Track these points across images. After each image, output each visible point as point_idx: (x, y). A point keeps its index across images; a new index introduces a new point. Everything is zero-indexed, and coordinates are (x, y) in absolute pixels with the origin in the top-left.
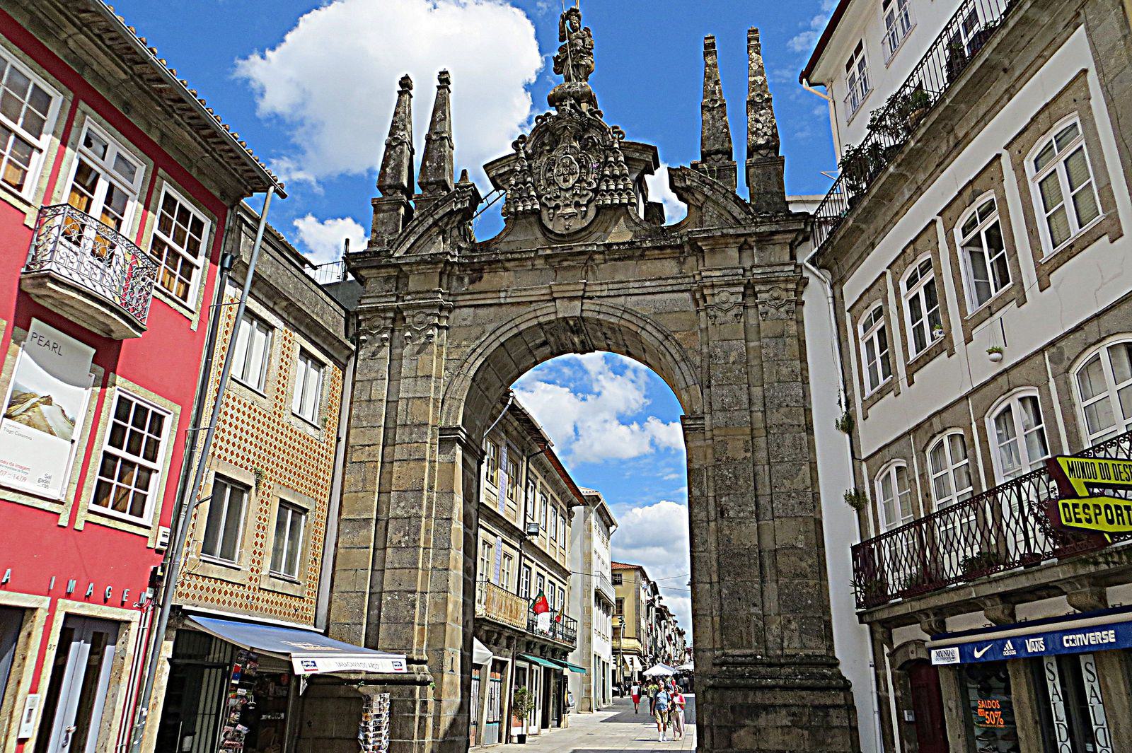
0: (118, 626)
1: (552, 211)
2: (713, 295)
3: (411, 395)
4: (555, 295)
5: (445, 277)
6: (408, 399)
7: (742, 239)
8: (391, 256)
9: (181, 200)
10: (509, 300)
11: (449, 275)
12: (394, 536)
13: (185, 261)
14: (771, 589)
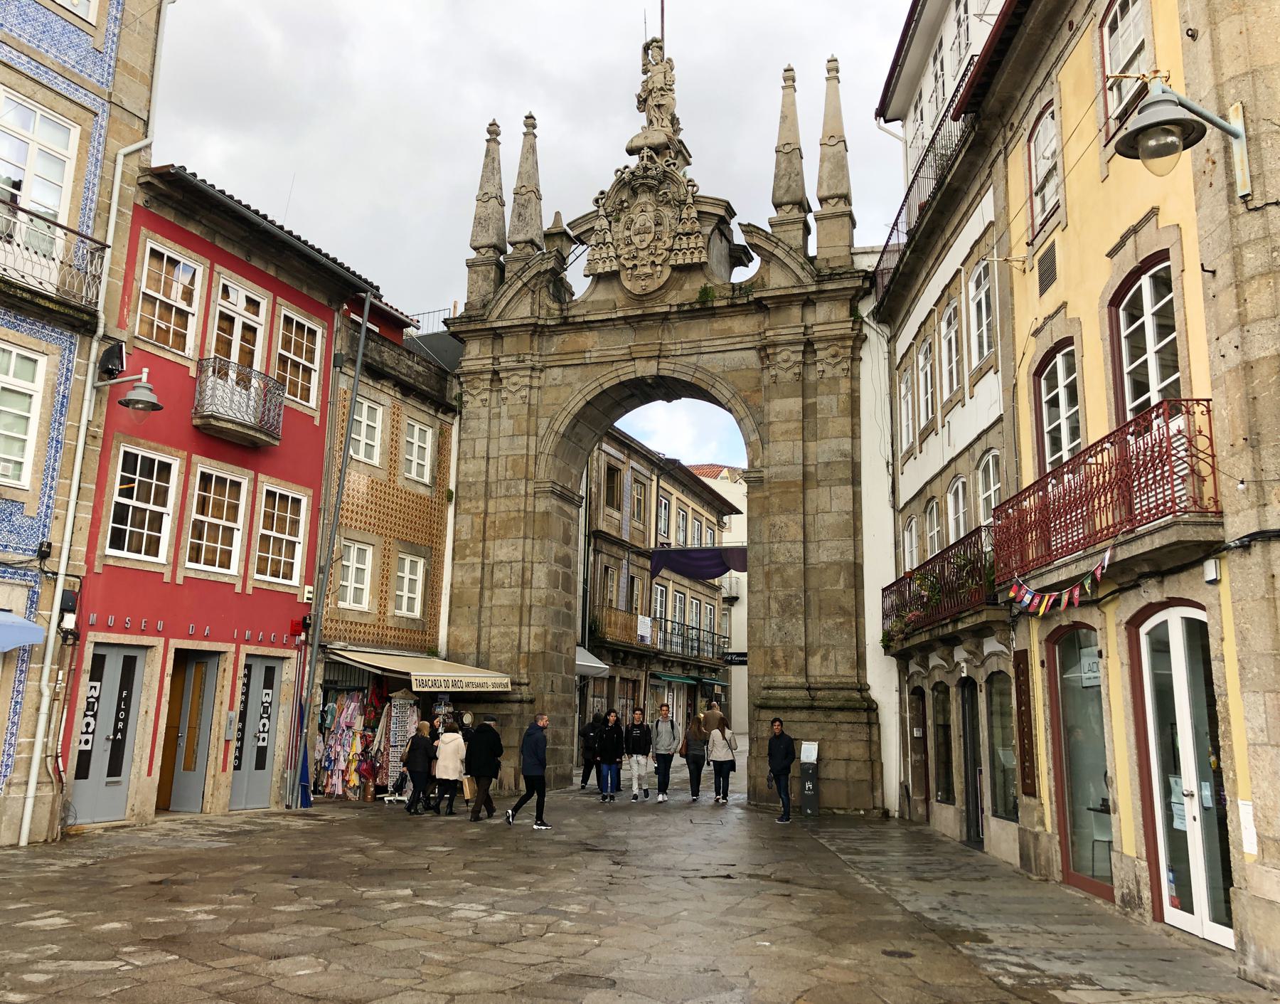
2: (775, 354)
4: (634, 356)
9: (297, 317)
10: (593, 360)
13: (305, 368)
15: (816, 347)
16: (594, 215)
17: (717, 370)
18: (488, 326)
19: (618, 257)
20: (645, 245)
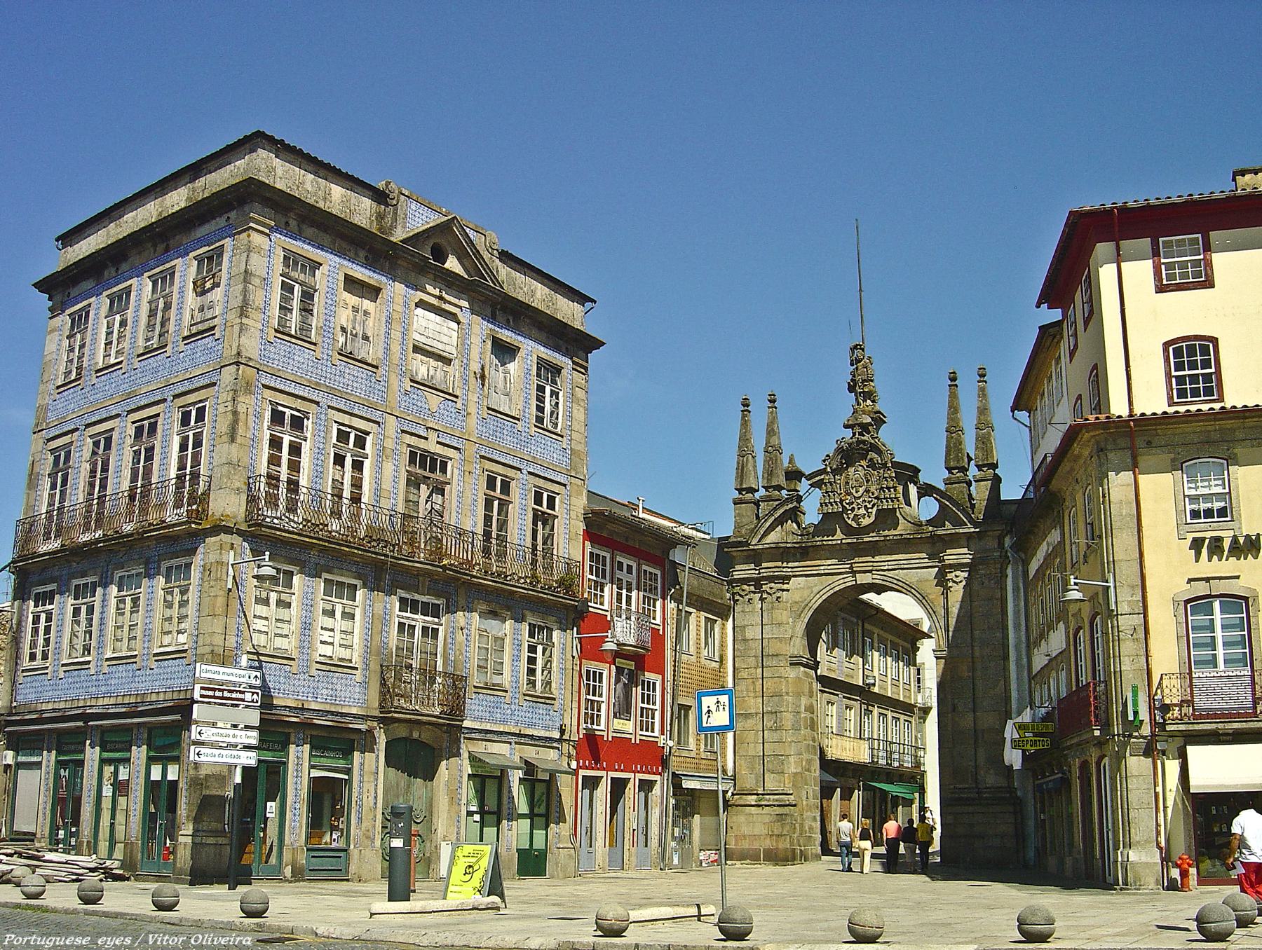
0: (652, 783)
1: (849, 512)
6: (769, 639)
12: (769, 724)
14: (981, 752)
16: (823, 472)
17: (914, 580)
18: (751, 547)
19: (841, 501)
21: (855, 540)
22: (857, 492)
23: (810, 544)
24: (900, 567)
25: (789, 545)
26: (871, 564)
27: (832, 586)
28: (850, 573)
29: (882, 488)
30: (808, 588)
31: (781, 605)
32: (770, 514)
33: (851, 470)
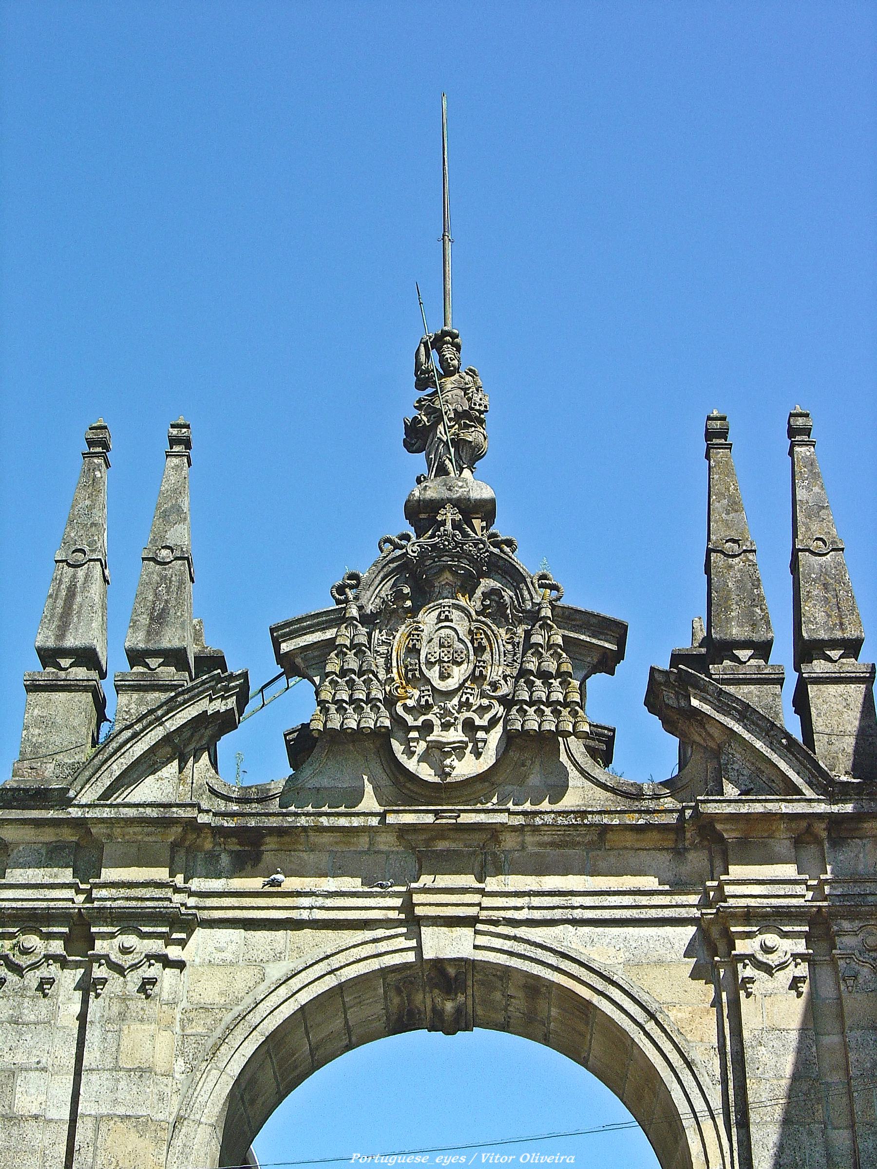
1: (414, 734)
3: (104, 1111)
4: (419, 911)
5: (182, 853)
7: (804, 824)
8: (68, 803)
11: (188, 850)
15: (836, 928)
18: (75, 812)
19: (390, 701)
20: (452, 684)
21: (429, 819)
22: (443, 677)
23: (274, 822)
24: (568, 914)
25: (203, 819)
26: (476, 898)
27: (335, 962)
28: (399, 923)
29: (523, 673)
30: (250, 962)
31: (152, 1009)
32: (150, 718)
33: (428, 619)
